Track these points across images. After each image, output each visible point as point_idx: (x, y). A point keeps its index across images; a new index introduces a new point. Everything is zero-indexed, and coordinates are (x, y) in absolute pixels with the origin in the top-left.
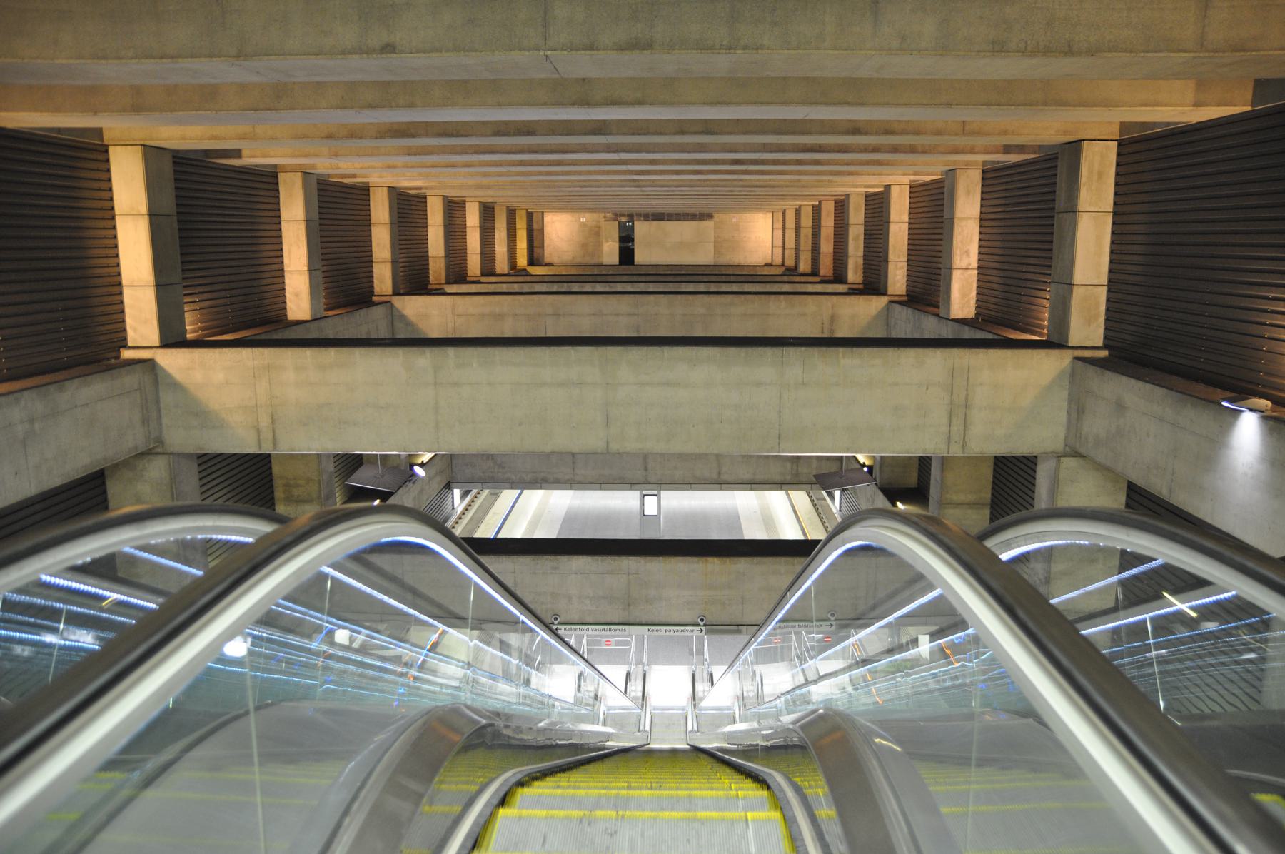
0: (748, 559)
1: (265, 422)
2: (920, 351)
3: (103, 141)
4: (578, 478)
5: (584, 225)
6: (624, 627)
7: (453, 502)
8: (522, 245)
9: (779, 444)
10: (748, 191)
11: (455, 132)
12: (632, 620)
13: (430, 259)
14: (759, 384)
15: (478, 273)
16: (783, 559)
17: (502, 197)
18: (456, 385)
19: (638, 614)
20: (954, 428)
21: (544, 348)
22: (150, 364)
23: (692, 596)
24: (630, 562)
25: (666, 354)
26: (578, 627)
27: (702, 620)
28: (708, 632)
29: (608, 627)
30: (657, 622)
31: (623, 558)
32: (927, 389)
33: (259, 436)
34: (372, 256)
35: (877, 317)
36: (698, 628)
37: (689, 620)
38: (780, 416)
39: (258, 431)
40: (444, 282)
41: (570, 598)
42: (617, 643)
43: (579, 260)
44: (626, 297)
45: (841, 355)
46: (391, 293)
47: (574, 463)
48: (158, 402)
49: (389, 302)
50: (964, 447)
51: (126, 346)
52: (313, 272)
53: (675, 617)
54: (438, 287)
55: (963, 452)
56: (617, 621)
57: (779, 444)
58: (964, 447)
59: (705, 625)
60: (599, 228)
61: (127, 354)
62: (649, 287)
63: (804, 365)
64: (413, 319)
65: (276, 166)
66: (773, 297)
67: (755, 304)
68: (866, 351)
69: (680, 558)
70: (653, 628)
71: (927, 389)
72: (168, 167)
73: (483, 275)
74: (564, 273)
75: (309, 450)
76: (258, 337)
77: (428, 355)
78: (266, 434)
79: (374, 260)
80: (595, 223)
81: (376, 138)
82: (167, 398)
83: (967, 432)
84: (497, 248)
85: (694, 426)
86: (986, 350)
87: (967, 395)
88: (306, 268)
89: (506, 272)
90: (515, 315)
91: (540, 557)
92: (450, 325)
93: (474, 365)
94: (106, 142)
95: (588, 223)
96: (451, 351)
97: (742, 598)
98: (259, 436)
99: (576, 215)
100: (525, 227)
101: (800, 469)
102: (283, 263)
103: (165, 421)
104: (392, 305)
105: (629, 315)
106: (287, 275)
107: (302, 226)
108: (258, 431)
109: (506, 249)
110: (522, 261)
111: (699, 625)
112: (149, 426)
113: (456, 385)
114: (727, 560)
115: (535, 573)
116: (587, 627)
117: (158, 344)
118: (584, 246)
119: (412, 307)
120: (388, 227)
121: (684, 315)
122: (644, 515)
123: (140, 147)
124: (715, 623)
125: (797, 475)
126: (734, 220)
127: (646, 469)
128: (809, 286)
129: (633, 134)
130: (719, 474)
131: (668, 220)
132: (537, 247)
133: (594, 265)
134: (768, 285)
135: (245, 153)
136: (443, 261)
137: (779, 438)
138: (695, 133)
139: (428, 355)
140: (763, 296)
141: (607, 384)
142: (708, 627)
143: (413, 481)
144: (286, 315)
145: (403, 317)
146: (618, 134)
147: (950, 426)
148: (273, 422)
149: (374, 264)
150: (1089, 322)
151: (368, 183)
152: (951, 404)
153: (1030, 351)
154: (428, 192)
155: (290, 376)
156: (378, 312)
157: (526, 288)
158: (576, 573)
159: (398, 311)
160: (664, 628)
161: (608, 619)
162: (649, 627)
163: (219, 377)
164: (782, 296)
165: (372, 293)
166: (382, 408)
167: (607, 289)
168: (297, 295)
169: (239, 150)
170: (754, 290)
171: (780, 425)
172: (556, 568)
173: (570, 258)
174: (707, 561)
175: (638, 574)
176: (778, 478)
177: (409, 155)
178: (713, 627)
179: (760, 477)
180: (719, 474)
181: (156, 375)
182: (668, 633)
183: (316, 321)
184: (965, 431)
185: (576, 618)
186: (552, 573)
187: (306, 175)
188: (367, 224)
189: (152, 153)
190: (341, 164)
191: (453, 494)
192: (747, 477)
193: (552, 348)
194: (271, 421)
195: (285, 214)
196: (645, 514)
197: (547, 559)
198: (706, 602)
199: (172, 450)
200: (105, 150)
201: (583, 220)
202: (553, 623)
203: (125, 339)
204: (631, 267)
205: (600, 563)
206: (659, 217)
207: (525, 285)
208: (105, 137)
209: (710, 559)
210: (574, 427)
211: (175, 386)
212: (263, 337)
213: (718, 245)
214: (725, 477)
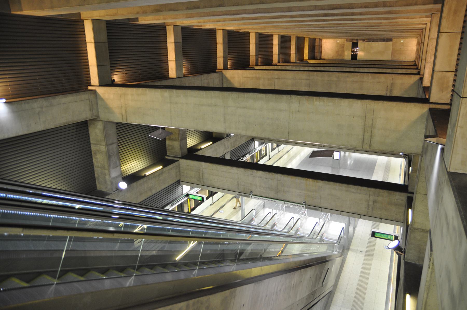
0: (324, 182)
1: (124, 112)
2: (351, 100)
3: (81, 18)
5: (338, 43)
6: (275, 200)
7: (255, 145)
8: (306, 51)
9: (288, 136)
10: (375, 28)
11: (174, 9)
12: (278, 198)
13: (250, 56)
14: (281, 110)
15: (277, 62)
16: (338, 184)
17: (294, 33)
18: (176, 103)
19: (280, 196)
20: (366, 137)
21: (203, 91)
22: (94, 92)
23: (301, 193)
25: (245, 96)
26: (258, 197)
27: (304, 203)
29: (269, 199)
30: (287, 200)
31: (276, 174)
32: (353, 118)
33: (122, 117)
34: (217, 55)
35: (414, 84)
36: (303, 205)
37: (299, 202)
38: (289, 125)
39: (122, 115)
40: (255, 65)
41: (256, 186)
43: (335, 58)
44: (306, 72)
45: (315, 100)
46: (223, 68)
48: (97, 104)
49: (221, 72)
50: (370, 146)
51: (91, 85)
52: (178, 61)
53: (294, 200)
54: (252, 67)
55: (370, 148)
56: (273, 197)
57: (288, 136)
58: (370, 146)
60: (344, 45)
61: (90, 88)
62: (330, 69)
63: (299, 103)
64: (229, 78)
65: (165, 23)
66: (366, 74)
67: (357, 77)
68: (326, 99)
69: (297, 177)
70: (285, 202)
71: (353, 118)
72: (104, 26)
73: (279, 62)
74: (321, 63)
75: (136, 123)
76: (145, 84)
77: (168, 92)
78: (124, 117)
79: (217, 57)
80: (342, 43)
81: (151, 13)
82: (99, 102)
83: (372, 139)
84: (291, 52)
85: (256, 125)
86: (382, 102)
87: (373, 122)
88: (174, 60)
89: (294, 62)
90: (264, 78)
91: (247, 169)
92: (241, 81)
93: (182, 96)
94: (82, 19)
95: (340, 43)
96: (174, 91)
97: (321, 197)
98: (122, 117)
99: (335, 39)
100: (308, 44)
102: (168, 57)
103: (100, 110)
104: (222, 74)
105: (306, 79)
106: (169, 62)
107: (173, 45)
108: (122, 115)
109: (295, 53)
110: (306, 57)
111: (303, 204)
112: (93, 111)
113: (176, 103)
114: (315, 181)
116: (262, 198)
117: (98, 85)
118: (337, 52)
119: (229, 74)
120: (222, 44)
121: (328, 81)
122: (334, 159)
123: (91, 20)
126: (402, 41)
128: (399, 70)
129: (233, 6)
131: (373, 42)
132: (317, 52)
133: (341, 60)
134: (381, 69)
135: (139, 19)
136: (255, 57)
137: (289, 134)
138: (257, 4)
139: (168, 92)
140: (361, 74)
141: (225, 106)
143: (229, 137)
144: (169, 76)
145: (226, 77)
146: (228, 6)
147: (364, 136)
148: (126, 113)
149: (217, 58)
150: (442, 90)
151: (215, 28)
152: (365, 125)
153: (405, 103)
154: (250, 31)
155: (130, 97)
156: (213, 76)
157: (306, 68)
159: (225, 75)
160: (290, 203)
161: (270, 196)
162: (284, 202)
163: (112, 97)
164: (370, 74)
165: (216, 68)
166: (155, 110)
167: (314, 69)
168: (172, 69)
169: (138, 18)
170: (374, 71)
171: (289, 128)
172: (251, 174)
173: (332, 57)
174: (307, 180)
177: (187, 18)
178: (308, 206)
181: (96, 95)
183: (179, 78)
184: (371, 138)
185: (258, 194)
186: (250, 176)
187: (175, 26)
188: (215, 43)
189: (95, 22)
190: (184, 22)
191: (255, 143)
193: (206, 91)
194: (125, 112)
195: (168, 41)
196: (334, 158)
198: (306, 196)
199: (101, 119)
200: (83, 21)
201: (338, 42)
202: (250, 194)
203: (90, 83)
204: (356, 61)
206: (370, 40)
207: (283, 67)
208: (81, 17)
209: (308, 179)
210: (214, 122)
211: (101, 99)
212: (148, 84)
213: (393, 52)
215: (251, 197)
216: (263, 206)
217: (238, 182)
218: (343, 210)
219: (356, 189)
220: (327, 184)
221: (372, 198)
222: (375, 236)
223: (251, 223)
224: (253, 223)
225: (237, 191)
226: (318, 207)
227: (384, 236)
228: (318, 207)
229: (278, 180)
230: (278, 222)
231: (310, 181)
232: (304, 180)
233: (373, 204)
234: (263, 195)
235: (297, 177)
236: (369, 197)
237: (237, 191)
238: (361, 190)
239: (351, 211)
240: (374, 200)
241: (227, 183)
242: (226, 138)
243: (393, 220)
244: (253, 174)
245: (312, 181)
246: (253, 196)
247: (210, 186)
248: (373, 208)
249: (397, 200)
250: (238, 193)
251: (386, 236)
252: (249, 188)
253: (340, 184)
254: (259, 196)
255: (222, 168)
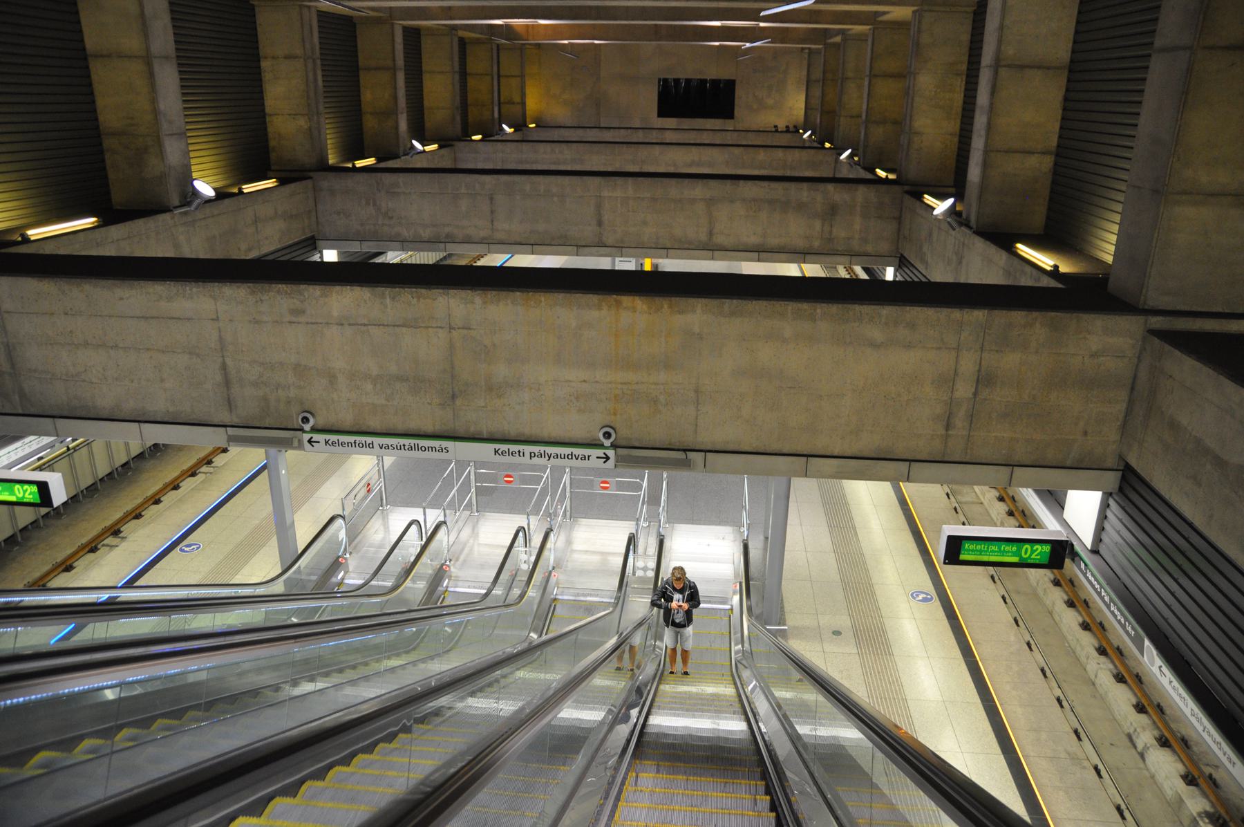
0: (712, 303)
4: (499, 236)
6: (444, 444)
19: (472, 415)
24: (452, 301)
26: (351, 439)
28: (620, 460)
29: (412, 441)
30: (513, 432)
31: (436, 292)
36: (600, 452)
37: (578, 433)
41: (332, 378)
42: (620, 486)
47: (492, 212)
53: (552, 428)
56: (429, 428)
59: (614, 446)
70: (504, 447)
91: (266, 286)
97: (697, 391)
101: (834, 230)
111: (601, 446)
115: (257, 322)
116: (369, 439)
124: (637, 444)
125: (830, 240)
127: (600, 224)
130: (711, 233)
142: (621, 451)
158: (342, 325)
160: (528, 449)
161: (413, 424)
162: (497, 446)
174: (618, 304)
175: (470, 329)
176: (800, 243)
179: (773, 241)
180: (711, 233)
182: (536, 460)
185: (346, 418)
192: (753, 240)
197: (279, 292)
205: (388, 301)
214: (720, 239)
215: (310, 441)
216: (382, 500)
217: (224, 367)
218: (820, 445)
219: (886, 324)
220: (732, 314)
221: (968, 364)
222: (963, 557)
223: (334, 580)
224: (343, 579)
225: (226, 417)
226: (685, 450)
227: (1003, 553)
228: (685, 450)
229: (451, 328)
230: (457, 560)
231: (634, 310)
232: (599, 308)
233: (975, 394)
234: (374, 423)
235: (561, 296)
236: (957, 357)
237: (227, 420)
238: (912, 326)
239: (868, 442)
240: (979, 371)
241: (162, 380)
242: (177, 212)
243: (1069, 463)
244: (303, 312)
245: (645, 307)
246: (316, 437)
247: (65, 413)
248: (971, 417)
249: (1094, 355)
250: (231, 431)
251: (1014, 549)
252: (293, 393)
253: (805, 306)
254: (354, 429)
255: (121, 299)
